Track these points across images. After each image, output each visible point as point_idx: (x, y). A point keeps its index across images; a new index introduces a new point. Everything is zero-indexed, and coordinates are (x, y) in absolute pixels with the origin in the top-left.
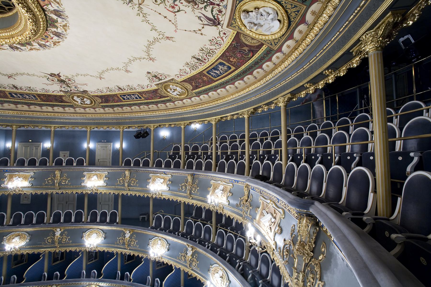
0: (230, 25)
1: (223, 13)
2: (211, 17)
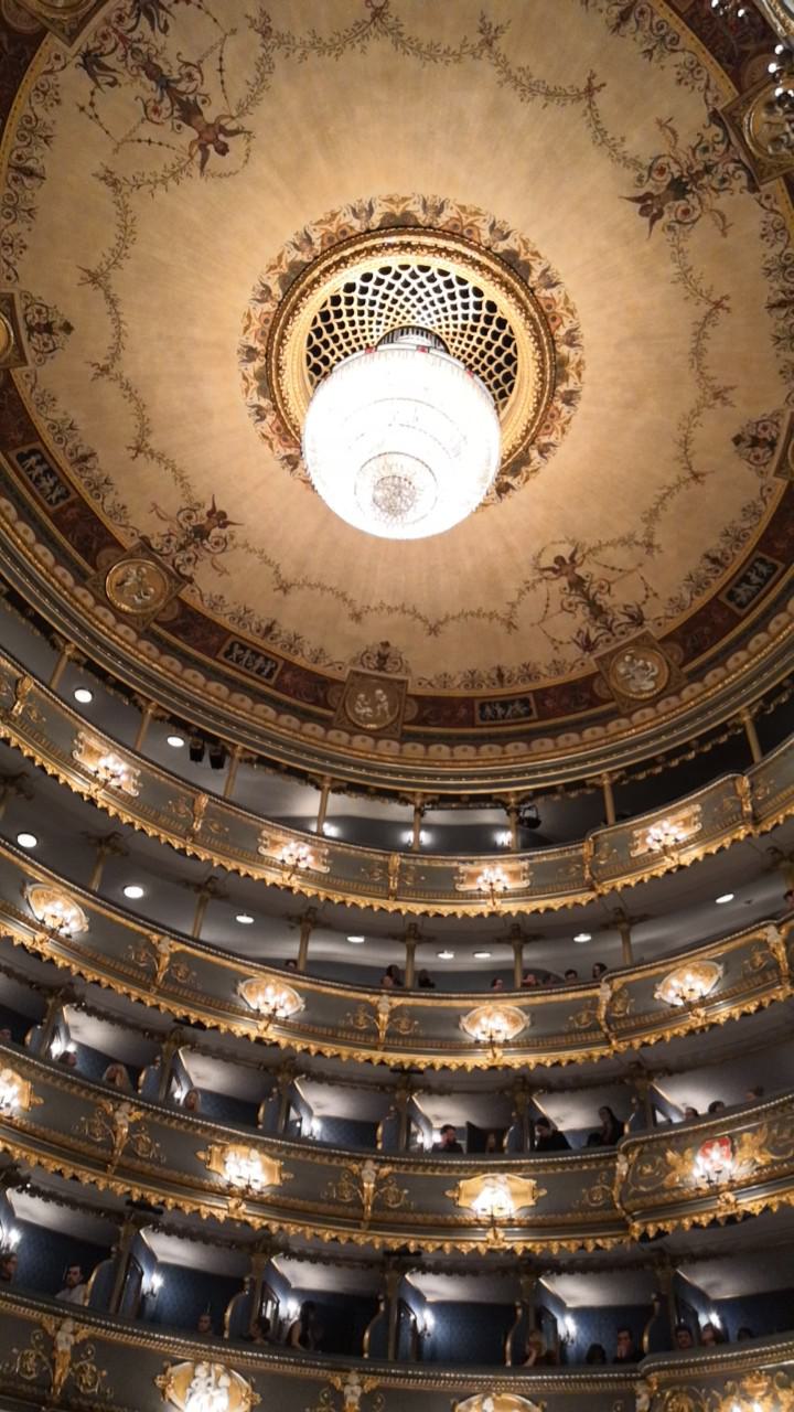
0: (600, 660)
2: (592, 639)
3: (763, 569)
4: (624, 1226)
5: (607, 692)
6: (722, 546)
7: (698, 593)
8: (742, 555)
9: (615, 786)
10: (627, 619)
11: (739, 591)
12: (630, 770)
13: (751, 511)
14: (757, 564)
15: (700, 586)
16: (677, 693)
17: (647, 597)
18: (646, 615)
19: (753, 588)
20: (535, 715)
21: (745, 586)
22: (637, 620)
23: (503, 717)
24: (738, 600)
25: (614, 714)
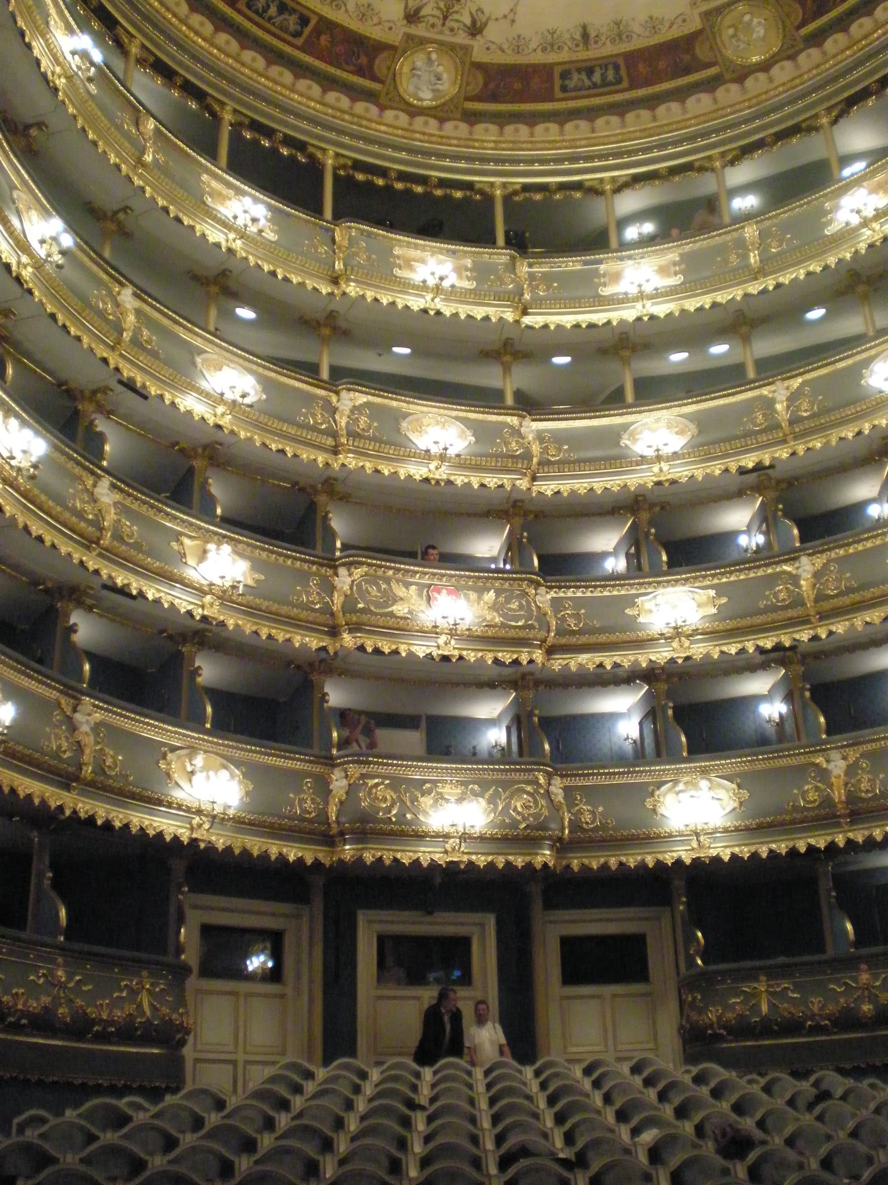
0: (409, 37)
1: (431, 29)
2: (423, 12)
3: (610, 75)
4: (334, 632)
5: (385, 71)
6: (604, 30)
7: (544, 50)
8: (609, 49)
9: (335, 169)
10: (468, 21)
11: (575, 76)
12: (358, 166)
13: (653, 24)
14: (610, 67)
15: (552, 45)
16: (442, 121)
17: (505, 17)
18: (485, 32)
19: (587, 83)
20: (299, 41)
21: (584, 76)
22: (475, 30)
23: (270, 19)
24: (567, 82)
25: (370, 96)
